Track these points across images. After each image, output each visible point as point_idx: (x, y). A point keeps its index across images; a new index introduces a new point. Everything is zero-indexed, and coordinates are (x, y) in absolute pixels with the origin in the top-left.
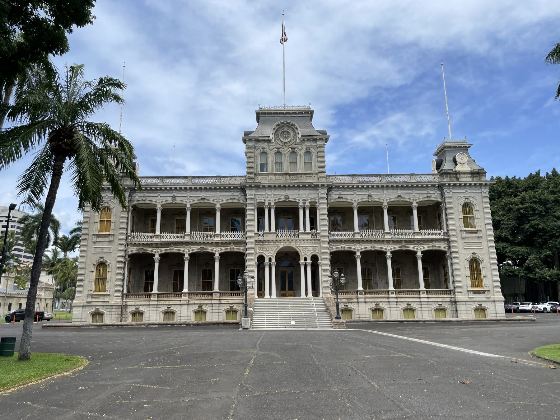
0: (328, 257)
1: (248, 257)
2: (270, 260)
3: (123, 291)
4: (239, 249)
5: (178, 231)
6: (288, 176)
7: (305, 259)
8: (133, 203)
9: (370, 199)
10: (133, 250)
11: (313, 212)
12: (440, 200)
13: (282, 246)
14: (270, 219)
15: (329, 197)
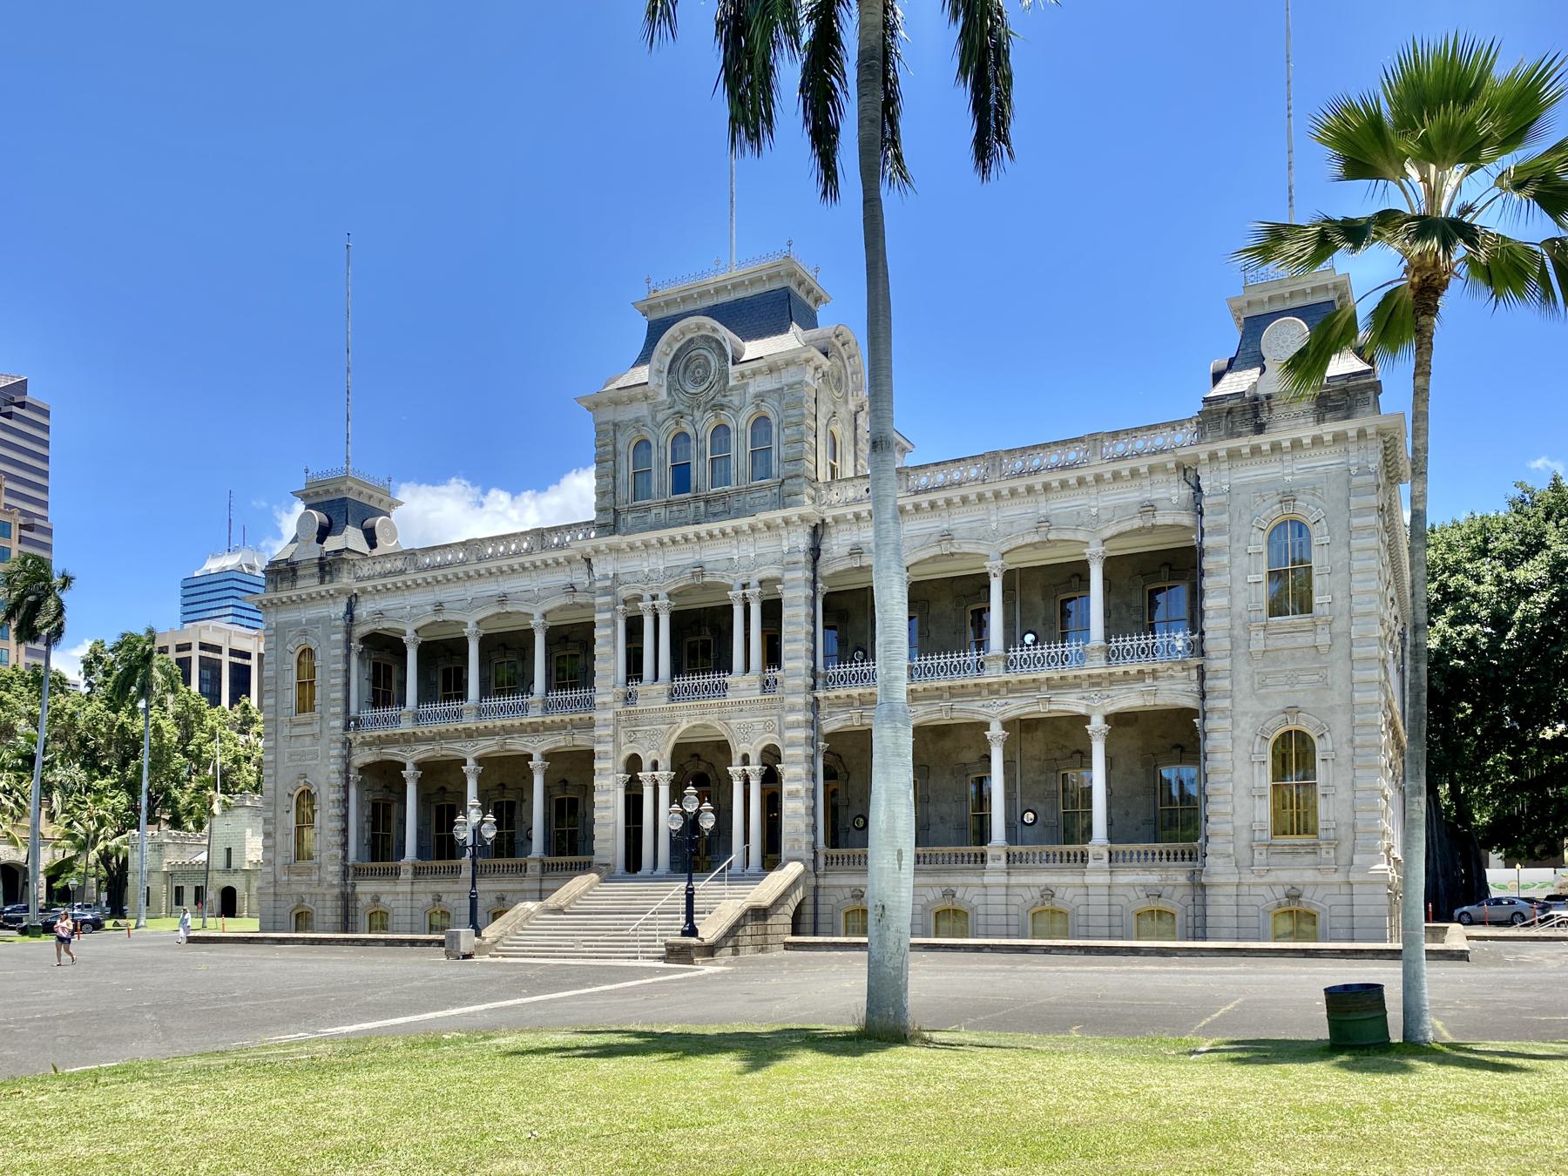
0: (800, 752)
1: (597, 765)
2: (655, 766)
3: (345, 857)
4: (581, 741)
5: (447, 698)
6: (702, 504)
7: (745, 760)
8: (361, 631)
9: (946, 548)
10: (363, 757)
11: (772, 611)
12: (1186, 520)
13: (684, 726)
14: (658, 647)
15: (823, 556)
